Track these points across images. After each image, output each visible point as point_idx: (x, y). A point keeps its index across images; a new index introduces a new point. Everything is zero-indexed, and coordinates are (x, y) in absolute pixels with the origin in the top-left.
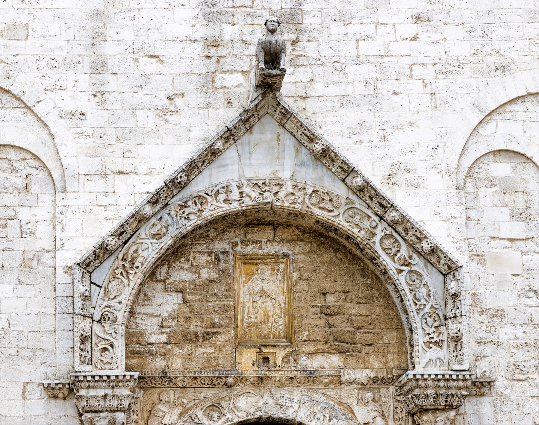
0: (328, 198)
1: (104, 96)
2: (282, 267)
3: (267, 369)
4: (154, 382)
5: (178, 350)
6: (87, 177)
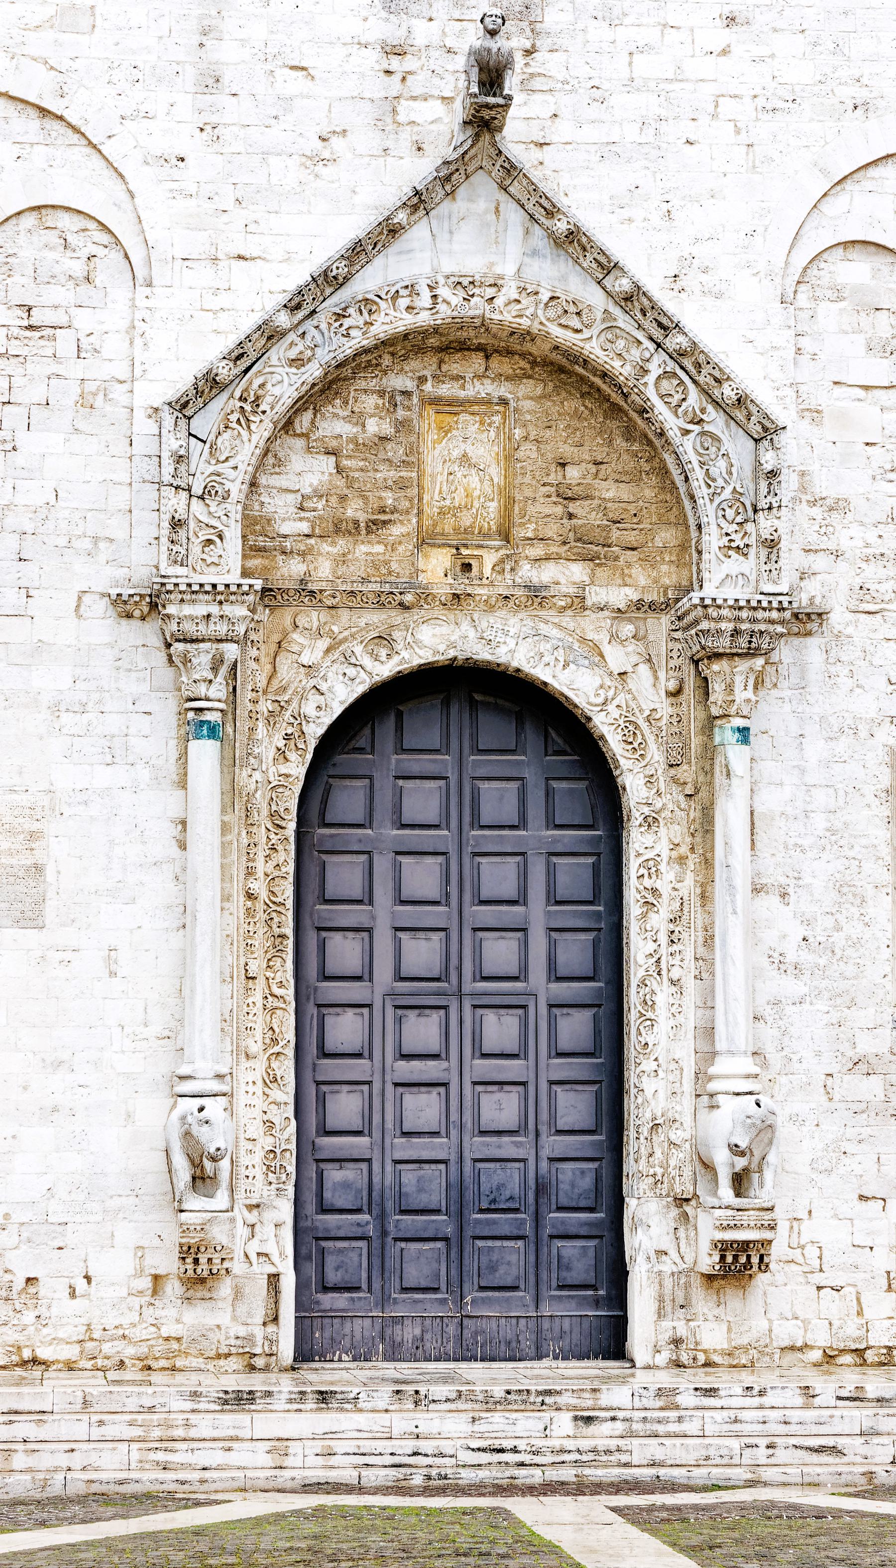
1: (216, 130)
2: (497, 419)
3: (467, 581)
4: (286, 597)
5: (326, 547)
6: (187, 263)
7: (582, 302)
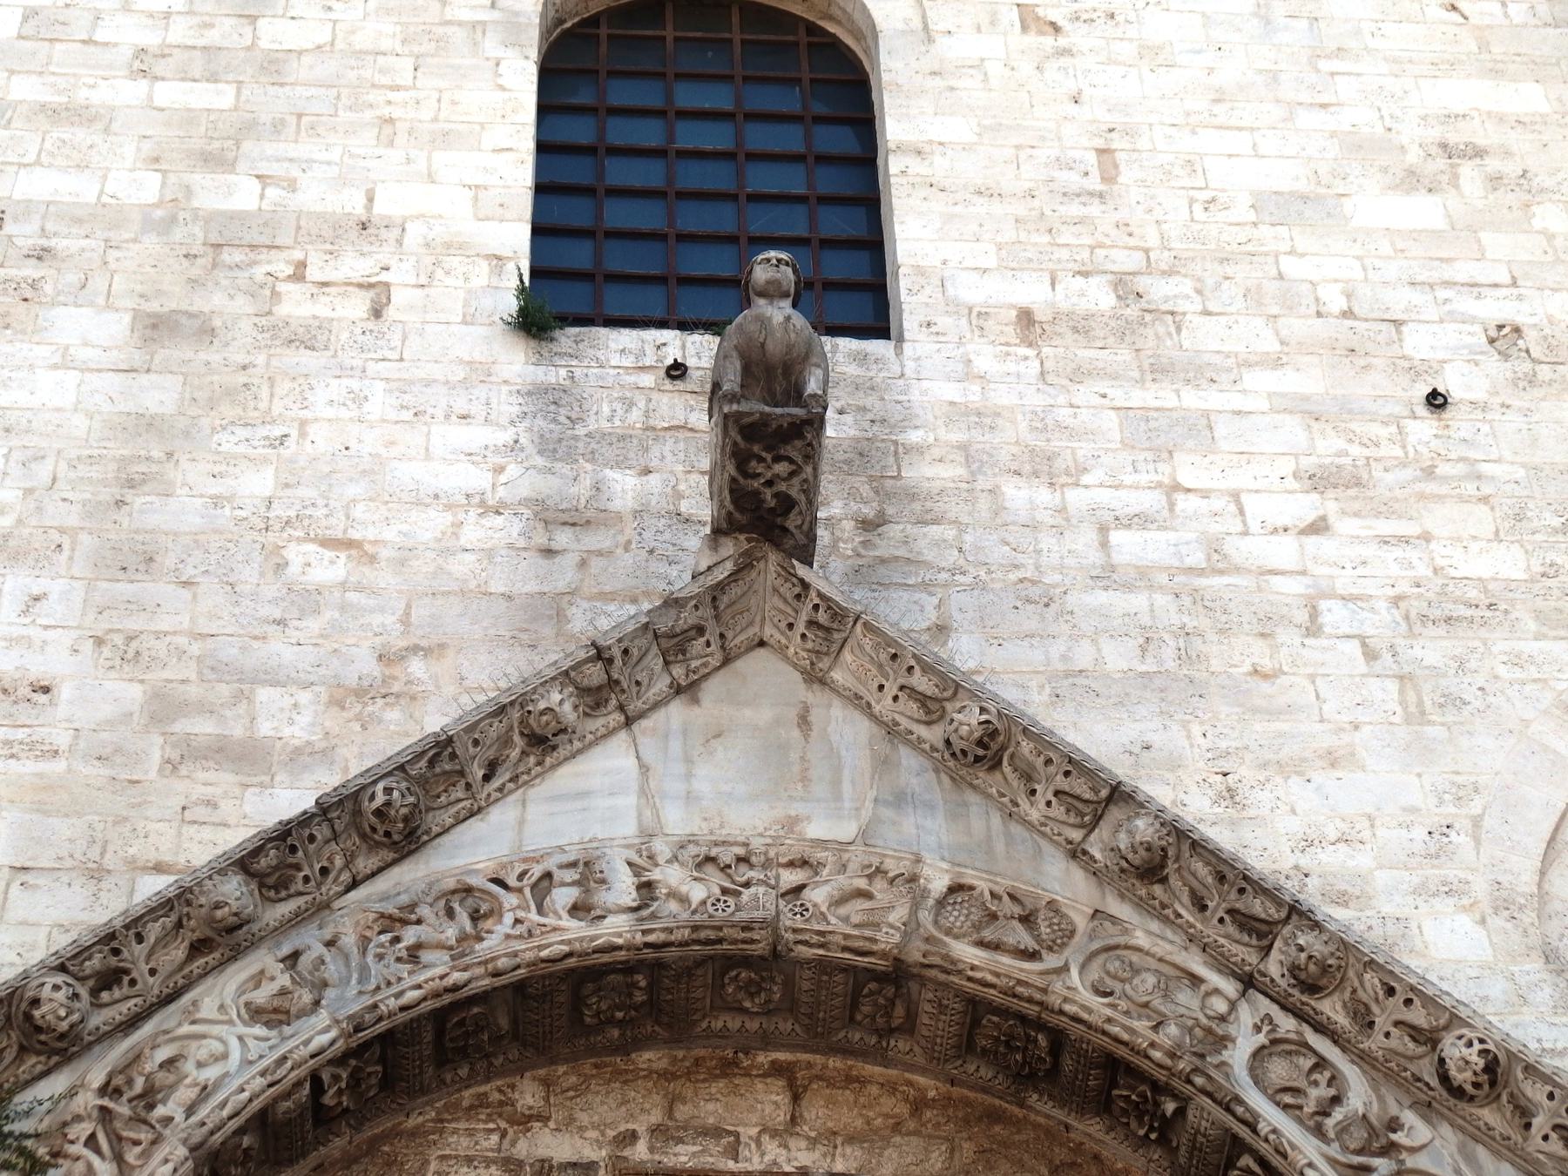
0: (1017, 910)
1: (134, 644)
7: (1038, 897)
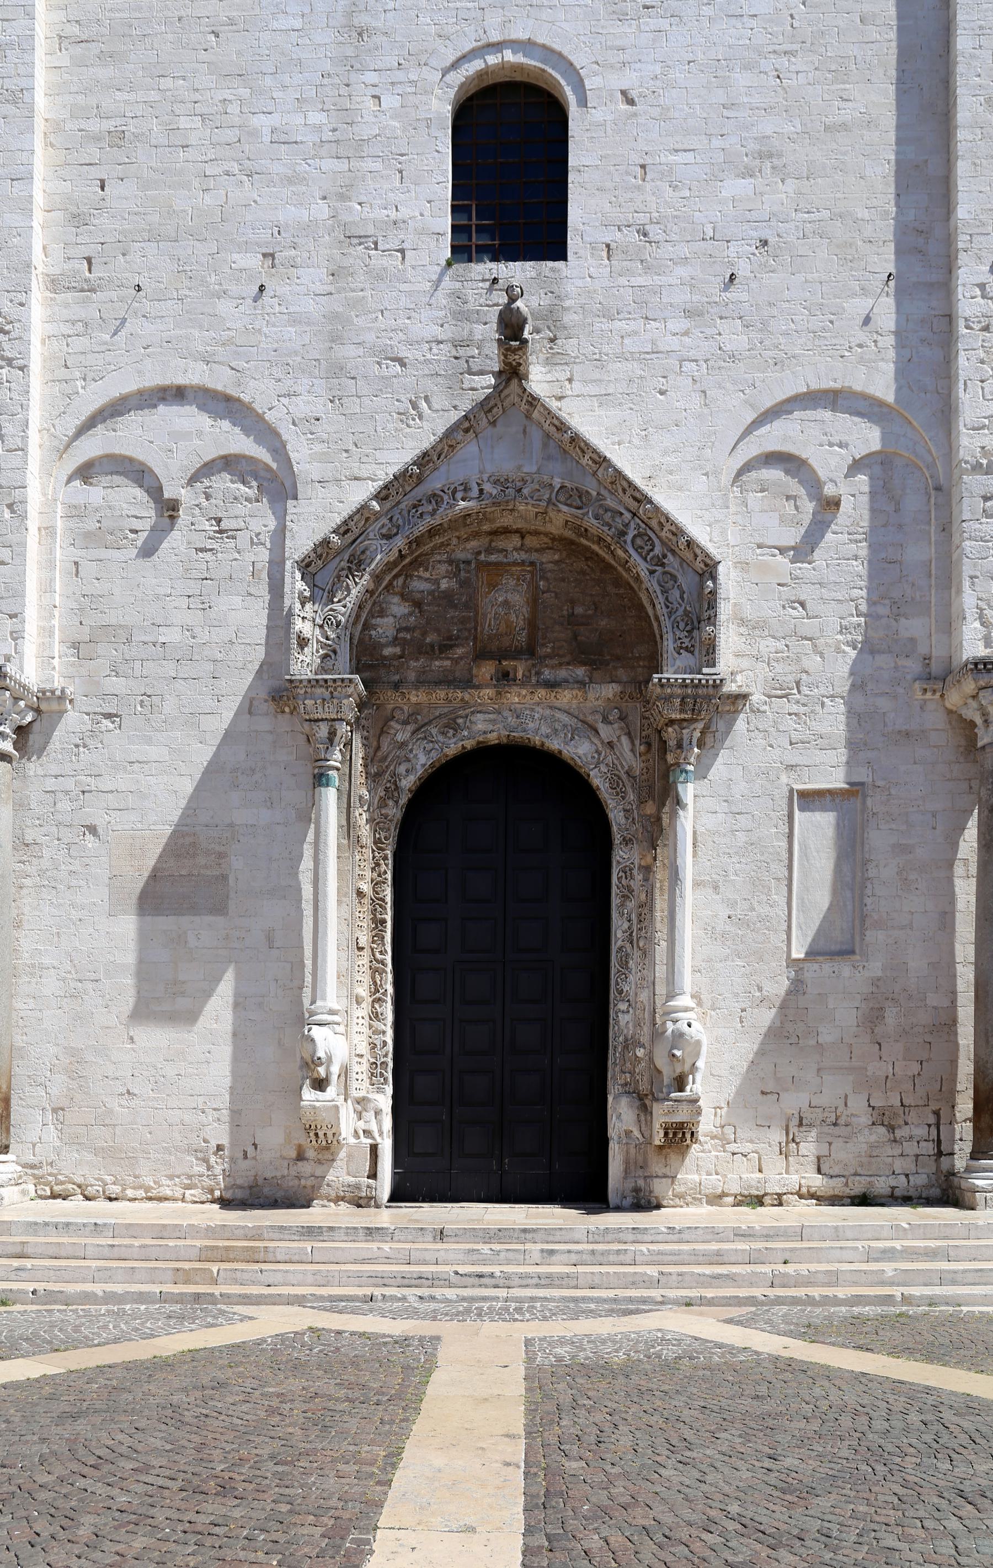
5: (413, 664)
